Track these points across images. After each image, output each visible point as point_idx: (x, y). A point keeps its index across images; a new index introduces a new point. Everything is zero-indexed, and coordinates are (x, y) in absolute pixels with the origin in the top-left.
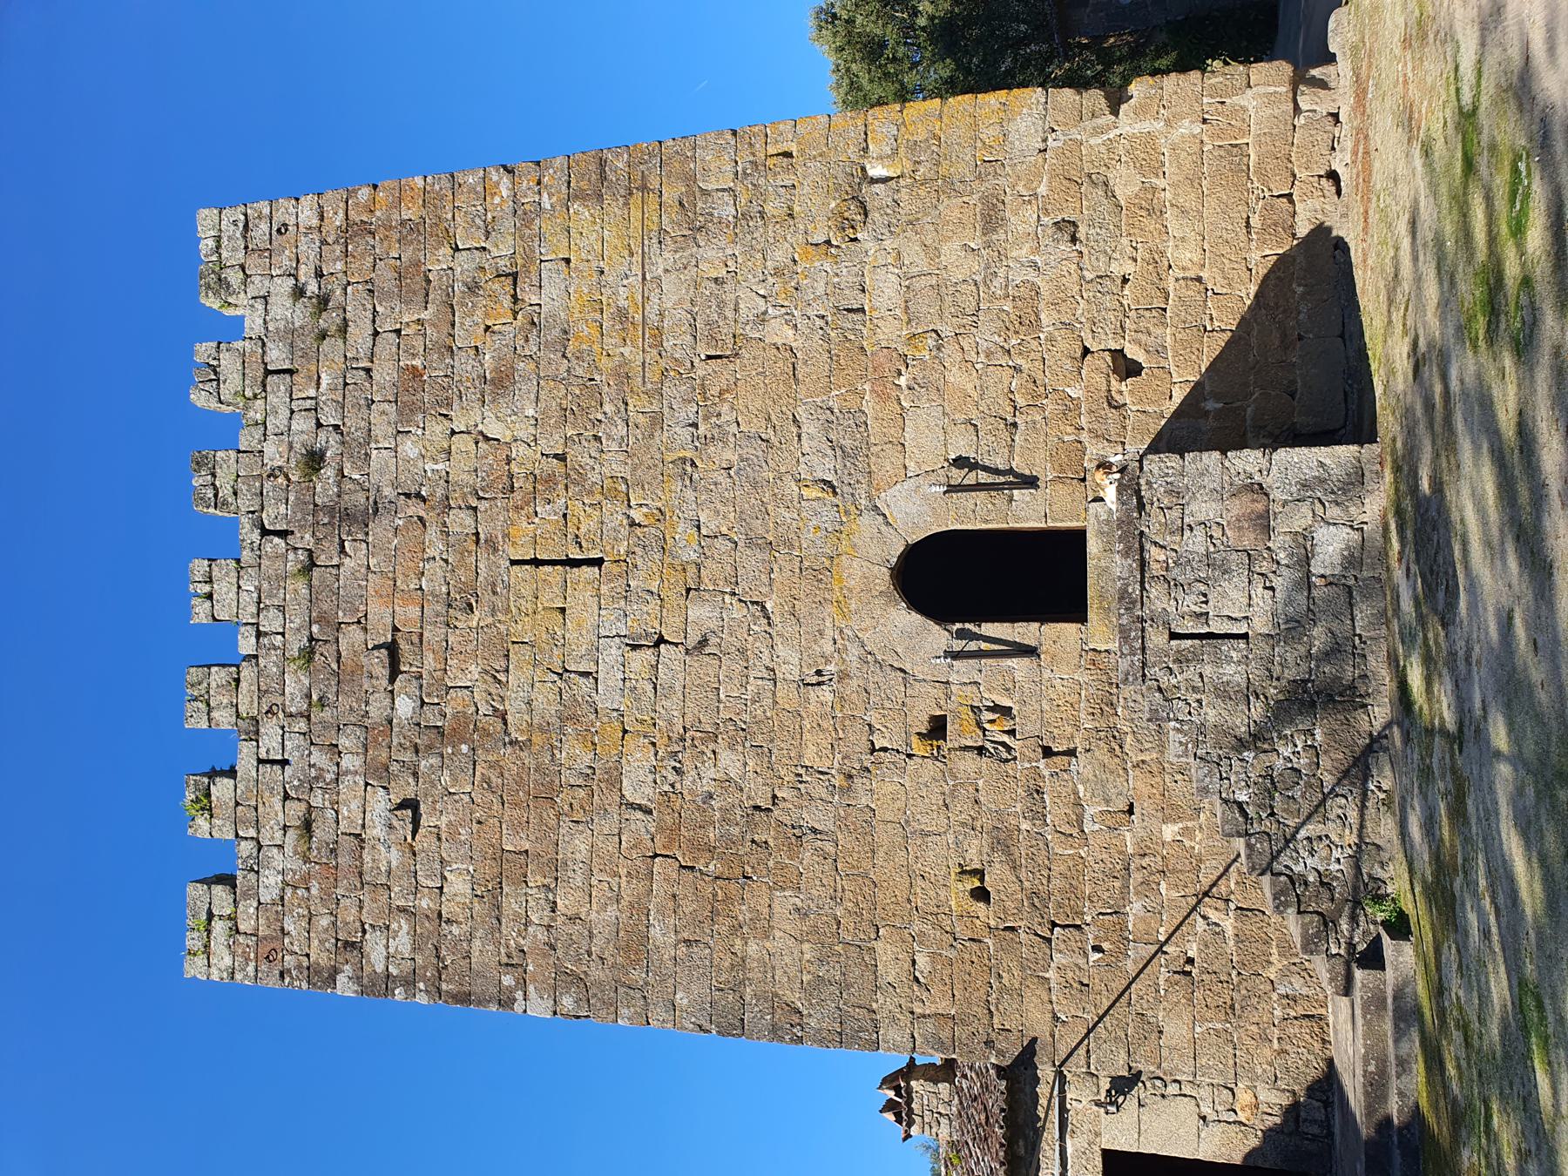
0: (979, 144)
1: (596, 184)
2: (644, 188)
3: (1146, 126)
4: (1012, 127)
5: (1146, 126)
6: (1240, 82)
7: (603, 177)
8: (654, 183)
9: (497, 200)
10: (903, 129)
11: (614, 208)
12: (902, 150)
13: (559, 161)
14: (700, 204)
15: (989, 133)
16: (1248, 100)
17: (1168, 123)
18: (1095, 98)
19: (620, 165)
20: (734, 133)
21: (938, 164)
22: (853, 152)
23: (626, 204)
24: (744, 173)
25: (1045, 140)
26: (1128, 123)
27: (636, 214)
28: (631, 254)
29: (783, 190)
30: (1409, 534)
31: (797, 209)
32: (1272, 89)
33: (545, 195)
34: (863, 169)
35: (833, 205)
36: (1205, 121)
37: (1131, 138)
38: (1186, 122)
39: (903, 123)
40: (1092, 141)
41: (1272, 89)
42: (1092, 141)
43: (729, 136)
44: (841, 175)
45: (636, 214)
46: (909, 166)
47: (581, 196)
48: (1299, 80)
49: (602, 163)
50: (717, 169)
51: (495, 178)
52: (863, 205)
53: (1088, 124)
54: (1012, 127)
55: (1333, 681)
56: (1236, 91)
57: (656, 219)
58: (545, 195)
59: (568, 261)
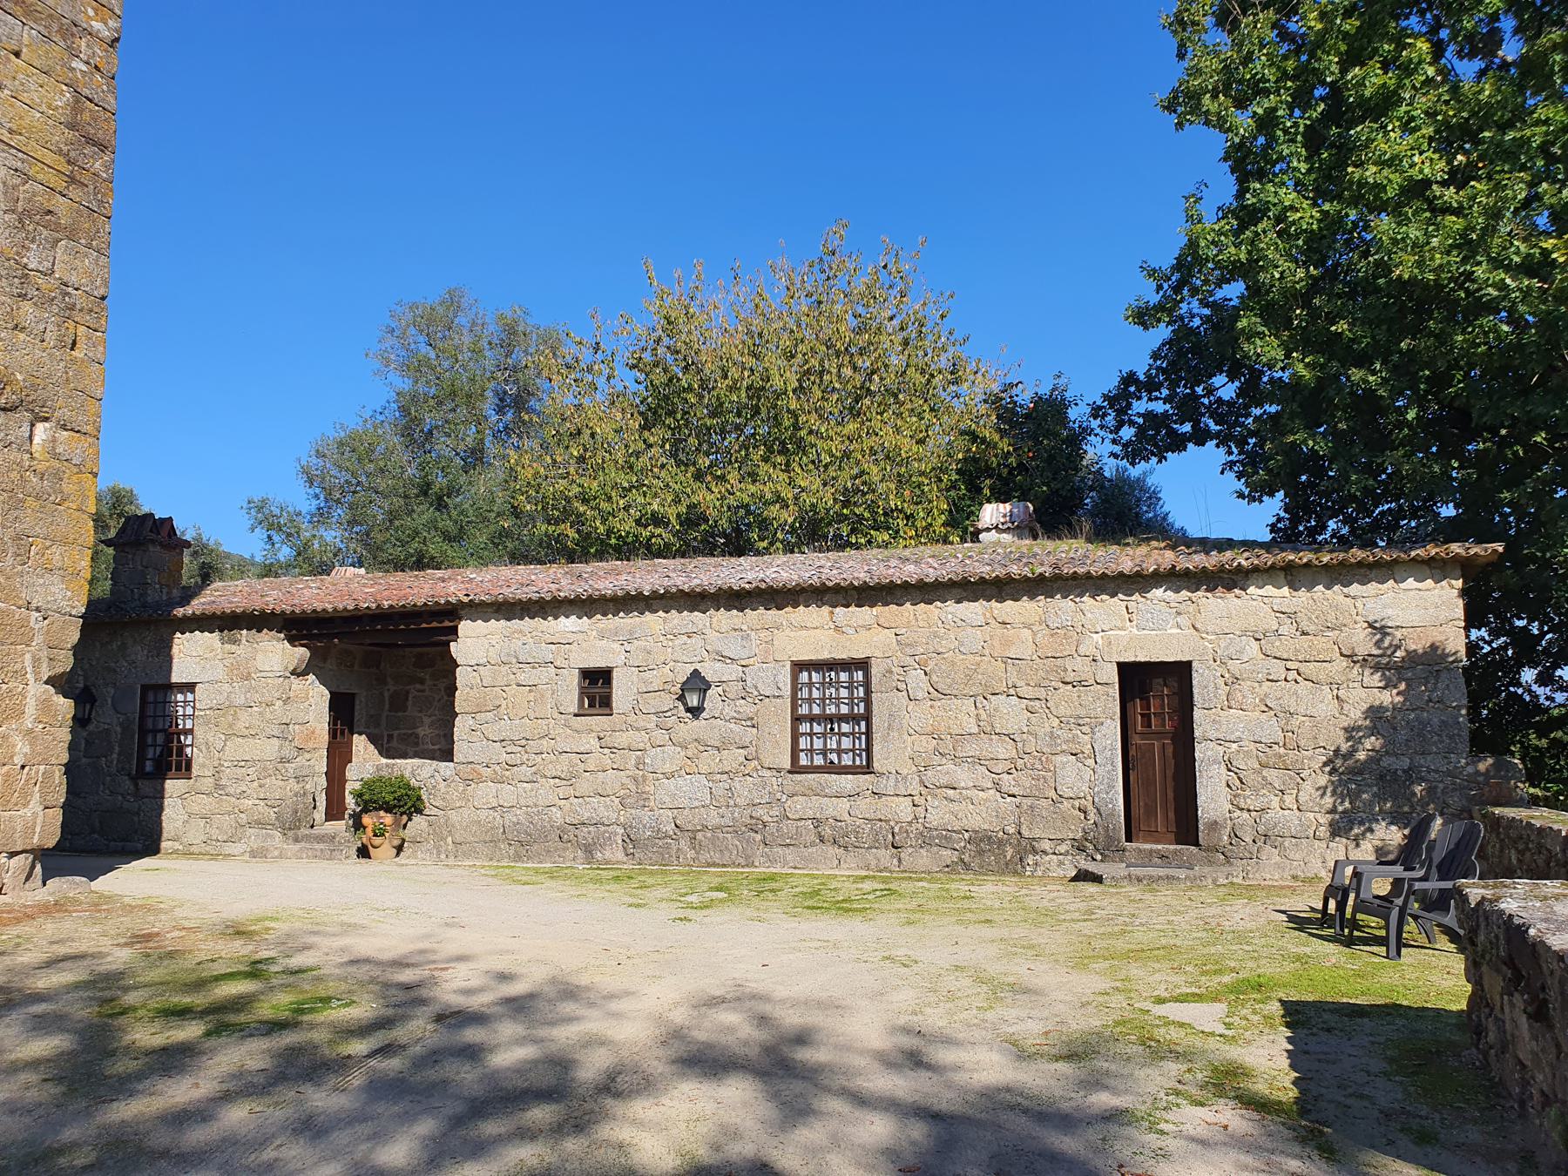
0: (48, 543)
1: (86, 133)
2: (72, 180)
3: (31, 709)
4: (56, 579)
5: (31, 709)
6: (51, 800)
7: (90, 141)
8: (75, 192)
9: (91, 12)
10: (75, 470)
11: (62, 136)
12: (56, 464)
13: (111, 102)
14: (45, 233)
15: (56, 554)
16: (35, 805)
17: (31, 731)
18: (66, 663)
19: (97, 165)
20: (103, 298)
21: (37, 498)
22: (64, 413)
23: (60, 152)
24: (68, 294)
25: (38, 610)
26: (36, 691)
27: (50, 158)
28: (11, 131)
29: (42, 328)
30: (1171, 815)
31: (22, 336)
32: (38, 829)
33: (84, 68)
34: (46, 419)
35: (19, 377)
36: (23, 767)
37: (23, 695)
38: (27, 749)
39: (81, 472)
40: (28, 656)
41: (38, 829)
42: (28, 656)
43: (102, 291)
44: (45, 395)
45: (50, 158)
46: (40, 467)
47: (76, 107)
48: (41, 854)
49: (103, 147)
50: (74, 266)
51: (111, 23)
52: (13, 409)
53: (44, 654)
54: (56, 579)
55: (398, 702)
56: (43, 795)
57: (40, 177)
58: (84, 68)
59: (17, 54)
